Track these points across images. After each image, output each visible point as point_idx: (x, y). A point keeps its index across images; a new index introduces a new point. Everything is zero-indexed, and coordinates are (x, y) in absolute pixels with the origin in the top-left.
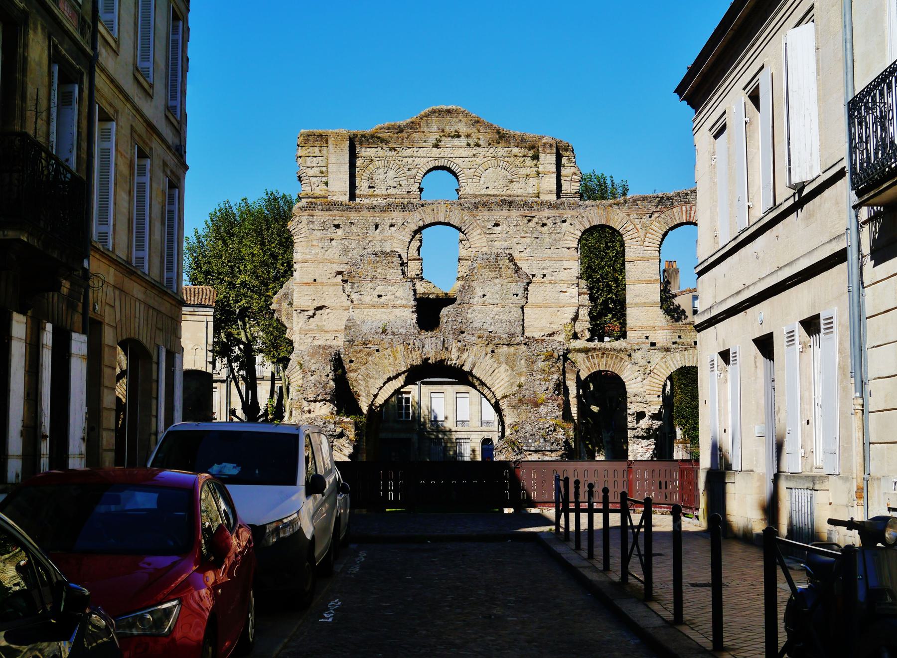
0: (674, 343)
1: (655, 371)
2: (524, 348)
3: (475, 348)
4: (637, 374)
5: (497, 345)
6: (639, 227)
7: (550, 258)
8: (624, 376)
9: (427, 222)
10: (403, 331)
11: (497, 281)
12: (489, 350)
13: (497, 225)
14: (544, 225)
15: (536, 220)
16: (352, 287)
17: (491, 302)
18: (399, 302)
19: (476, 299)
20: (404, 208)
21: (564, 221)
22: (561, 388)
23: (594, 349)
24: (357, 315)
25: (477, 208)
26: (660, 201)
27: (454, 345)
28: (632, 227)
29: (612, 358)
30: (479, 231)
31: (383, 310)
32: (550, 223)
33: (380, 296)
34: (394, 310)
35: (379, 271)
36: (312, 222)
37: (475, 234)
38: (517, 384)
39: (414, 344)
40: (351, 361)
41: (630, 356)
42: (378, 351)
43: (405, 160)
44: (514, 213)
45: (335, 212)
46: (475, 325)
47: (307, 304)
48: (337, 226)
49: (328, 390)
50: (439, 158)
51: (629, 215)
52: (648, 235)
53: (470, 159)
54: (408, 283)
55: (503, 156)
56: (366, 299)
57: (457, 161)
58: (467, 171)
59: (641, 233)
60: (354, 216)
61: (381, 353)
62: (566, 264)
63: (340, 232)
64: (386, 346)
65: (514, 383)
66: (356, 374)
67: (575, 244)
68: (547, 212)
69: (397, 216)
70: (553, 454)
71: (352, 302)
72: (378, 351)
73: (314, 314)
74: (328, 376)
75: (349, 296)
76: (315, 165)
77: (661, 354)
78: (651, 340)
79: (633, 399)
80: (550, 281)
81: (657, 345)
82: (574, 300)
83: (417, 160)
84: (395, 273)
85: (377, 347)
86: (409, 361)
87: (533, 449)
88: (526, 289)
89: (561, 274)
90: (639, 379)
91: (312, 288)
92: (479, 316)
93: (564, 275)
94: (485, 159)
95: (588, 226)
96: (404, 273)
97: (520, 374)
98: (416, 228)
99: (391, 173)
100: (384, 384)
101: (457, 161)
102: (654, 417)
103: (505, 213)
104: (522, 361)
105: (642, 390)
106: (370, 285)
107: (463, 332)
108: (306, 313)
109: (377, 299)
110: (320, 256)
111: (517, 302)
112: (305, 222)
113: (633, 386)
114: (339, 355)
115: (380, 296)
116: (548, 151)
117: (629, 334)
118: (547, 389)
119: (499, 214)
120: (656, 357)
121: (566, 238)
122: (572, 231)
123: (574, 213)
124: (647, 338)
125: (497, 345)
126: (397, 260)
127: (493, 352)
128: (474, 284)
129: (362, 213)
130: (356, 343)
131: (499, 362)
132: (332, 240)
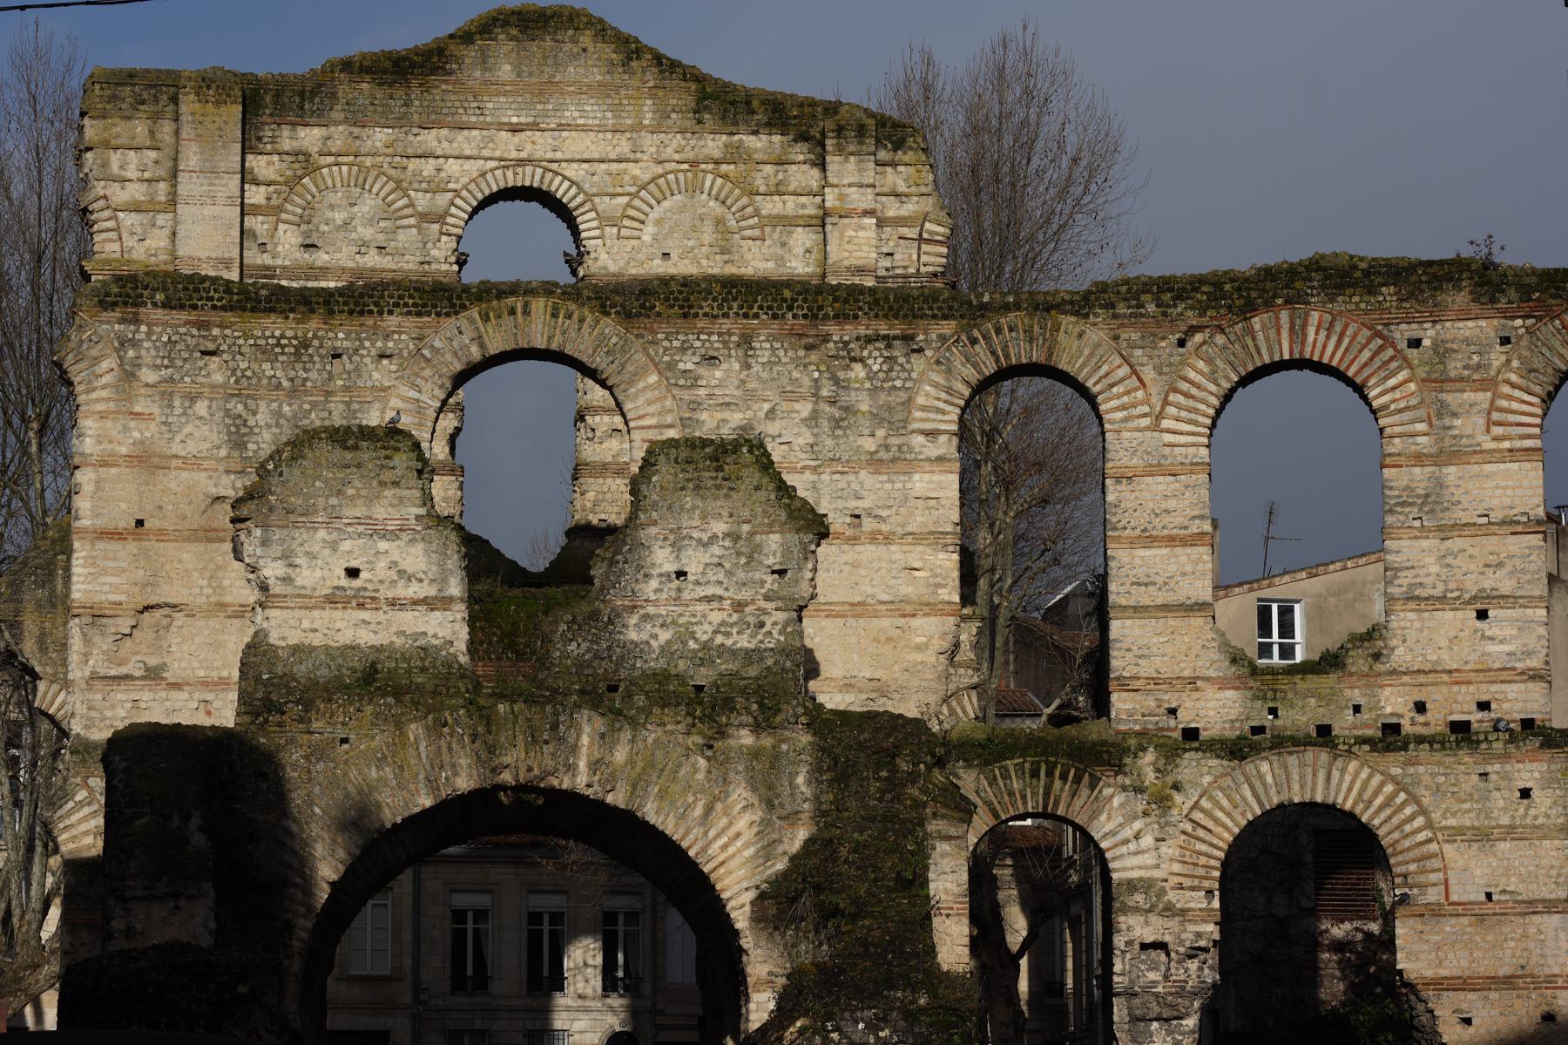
4: (1137, 825)
6: (1148, 373)
7: (875, 463)
8: (1102, 829)
9: (494, 349)
11: (720, 527)
13: (710, 360)
17: (701, 592)
18: (415, 590)
19: (654, 583)
24: (287, 628)
27: (587, 729)
31: (364, 615)
35: (350, 492)
43: (413, 165)
47: (114, 598)
50: (521, 162)
51: (1116, 338)
52: (1171, 398)
53: (614, 166)
58: (603, 203)
69: (400, 328)
78: (1186, 718)
81: (1204, 735)
83: (453, 166)
90: (1147, 841)
91: (132, 546)
95: (990, 368)
97: (792, 818)
98: (458, 366)
99: (368, 205)
101: (572, 171)
104: (800, 780)
113: (1128, 862)
115: (353, 573)
117: (1120, 702)
121: (920, 400)
124: (1172, 712)
126: (403, 461)
132: (193, 399)
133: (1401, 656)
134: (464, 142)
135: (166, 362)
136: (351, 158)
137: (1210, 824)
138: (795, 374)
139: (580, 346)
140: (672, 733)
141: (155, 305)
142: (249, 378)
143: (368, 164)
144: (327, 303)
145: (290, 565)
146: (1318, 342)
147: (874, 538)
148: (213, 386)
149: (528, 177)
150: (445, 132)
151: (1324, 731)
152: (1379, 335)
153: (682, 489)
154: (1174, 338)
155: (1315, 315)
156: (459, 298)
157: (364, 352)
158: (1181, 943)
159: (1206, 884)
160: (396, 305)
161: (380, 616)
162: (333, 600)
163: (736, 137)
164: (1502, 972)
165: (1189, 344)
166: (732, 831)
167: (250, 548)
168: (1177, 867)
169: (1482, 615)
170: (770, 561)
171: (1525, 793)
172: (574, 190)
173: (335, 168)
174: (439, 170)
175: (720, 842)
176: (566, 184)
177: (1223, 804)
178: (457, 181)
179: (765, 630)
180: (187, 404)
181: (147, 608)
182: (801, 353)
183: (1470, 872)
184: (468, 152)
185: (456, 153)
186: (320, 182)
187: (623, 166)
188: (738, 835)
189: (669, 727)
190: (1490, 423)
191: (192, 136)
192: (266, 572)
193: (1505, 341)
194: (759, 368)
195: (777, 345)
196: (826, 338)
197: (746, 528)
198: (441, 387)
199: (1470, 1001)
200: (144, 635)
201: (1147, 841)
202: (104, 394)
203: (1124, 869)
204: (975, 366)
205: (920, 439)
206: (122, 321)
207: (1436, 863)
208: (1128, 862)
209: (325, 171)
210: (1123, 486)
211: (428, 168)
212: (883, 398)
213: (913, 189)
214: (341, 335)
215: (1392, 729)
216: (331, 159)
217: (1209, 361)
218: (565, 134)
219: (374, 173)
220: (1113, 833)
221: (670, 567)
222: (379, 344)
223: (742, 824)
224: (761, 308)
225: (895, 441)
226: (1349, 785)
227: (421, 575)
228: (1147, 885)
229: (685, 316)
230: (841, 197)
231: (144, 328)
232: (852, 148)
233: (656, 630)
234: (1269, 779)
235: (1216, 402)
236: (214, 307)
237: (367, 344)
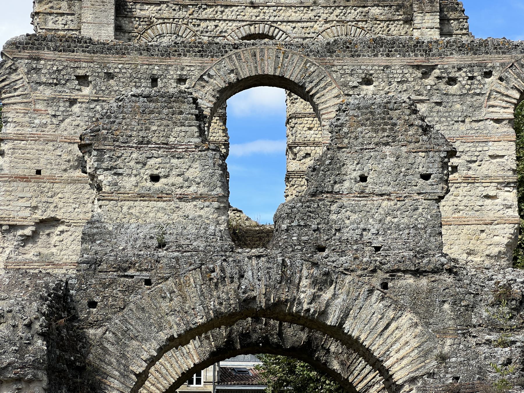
2: (449, 279)
3: (348, 279)
5: (393, 273)
9: (245, 73)
10: (200, 244)
11: (387, 150)
12: (376, 282)
13: (368, 81)
14: (452, 81)
15: (436, 72)
16: (100, 160)
19: (347, 184)
20: (201, 50)
21: (488, 74)
25: (331, 52)
27: (305, 273)
30: (335, 92)
31: (161, 204)
32: (462, 76)
33: (155, 178)
34: (182, 204)
36: (37, 70)
37: (328, 96)
38: (436, 352)
39: (223, 270)
40: (93, 304)
42: (148, 282)
43: (203, 25)
44: (397, 61)
45: (79, 55)
46: (346, 234)
48: (83, 80)
49: (29, 358)
53: (305, 25)
54: (210, 153)
55: (355, 20)
56: (128, 183)
57: (283, 27)
60: (114, 63)
61: (155, 288)
62: (493, 148)
63: (87, 91)
64: (166, 273)
65: (430, 351)
66: (100, 331)
67: (509, 113)
68: (455, 59)
69: (191, 64)
71: (99, 188)
72: (148, 282)
73: (35, 233)
74: (29, 326)
75: (93, 176)
76: (60, 27)
80: (467, 178)
83: (222, 26)
84: (185, 134)
85: (146, 275)
86: (212, 304)
89: (485, 165)
92: (354, 217)
93: (489, 168)
94: (328, 25)
96: (202, 133)
97: (444, 333)
98: (223, 85)
100: (162, 351)
101: (283, 27)
103: (382, 60)
104: (446, 306)
106: (134, 156)
107: (322, 249)
108: (20, 232)
109: (149, 184)
110: (49, 131)
111: (429, 189)
112: (22, 70)
114: (67, 290)
115: (155, 178)
116: (428, 9)
118: (509, 362)
119: (371, 63)
121: (491, 103)
122: (503, 90)
123: (507, 59)
125: (393, 273)
127: (385, 286)
128: (342, 155)
129: (127, 58)
130: (104, 266)
131: (402, 308)
132: (73, 102)
134: (229, 13)
135: (55, 81)
136: (172, 20)
138: (417, 88)
139: (293, 74)
140: (361, 276)
141: (49, 49)
142: (103, 91)
143: (180, 23)
144: (148, 50)
145: (115, 174)
148: (84, 96)
149: (260, 29)
150: (219, 8)
153: (362, 125)
156: (224, 47)
157: (170, 77)
160: (189, 51)
161: (173, 205)
162: (142, 196)
163: (366, 9)
166: (402, 341)
167: (91, 162)
170: (421, 169)
172: (284, 36)
173: (163, 25)
174: (216, 26)
175: (395, 347)
176: (281, 32)
178: (225, 32)
179: (417, 212)
180: (67, 104)
181: (42, 221)
182: (420, 75)
184: (230, 18)
185: (224, 18)
186: (155, 31)
187: (309, 24)
188: (407, 343)
189: (359, 272)
191: (89, 5)
192: (100, 178)
194: (395, 84)
195: (406, 71)
196: (434, 67)
197: (404, 149)
198: (213, 96)
200: (42, 238)
202: (18, 99)
205: (492, 122)
206: (31, 58)
209: (158, 26)
211: (211, 25)
212: (469, 98)
213: (459, 32)
214: (157, 68)
216: (161, 21)
218: (279, 8)
219: (184, 27)
221: (356, 174)
222: (179, 73)
223: (408, 336)
224: (396, 51)
225: (474, 125)
227: (198, 180)
229: (353, 56)
230: (422, 34)
231: (42, 62)
232: (428, 9)
233: (349, 213)
236: (83, 51)
237: (172, 73)
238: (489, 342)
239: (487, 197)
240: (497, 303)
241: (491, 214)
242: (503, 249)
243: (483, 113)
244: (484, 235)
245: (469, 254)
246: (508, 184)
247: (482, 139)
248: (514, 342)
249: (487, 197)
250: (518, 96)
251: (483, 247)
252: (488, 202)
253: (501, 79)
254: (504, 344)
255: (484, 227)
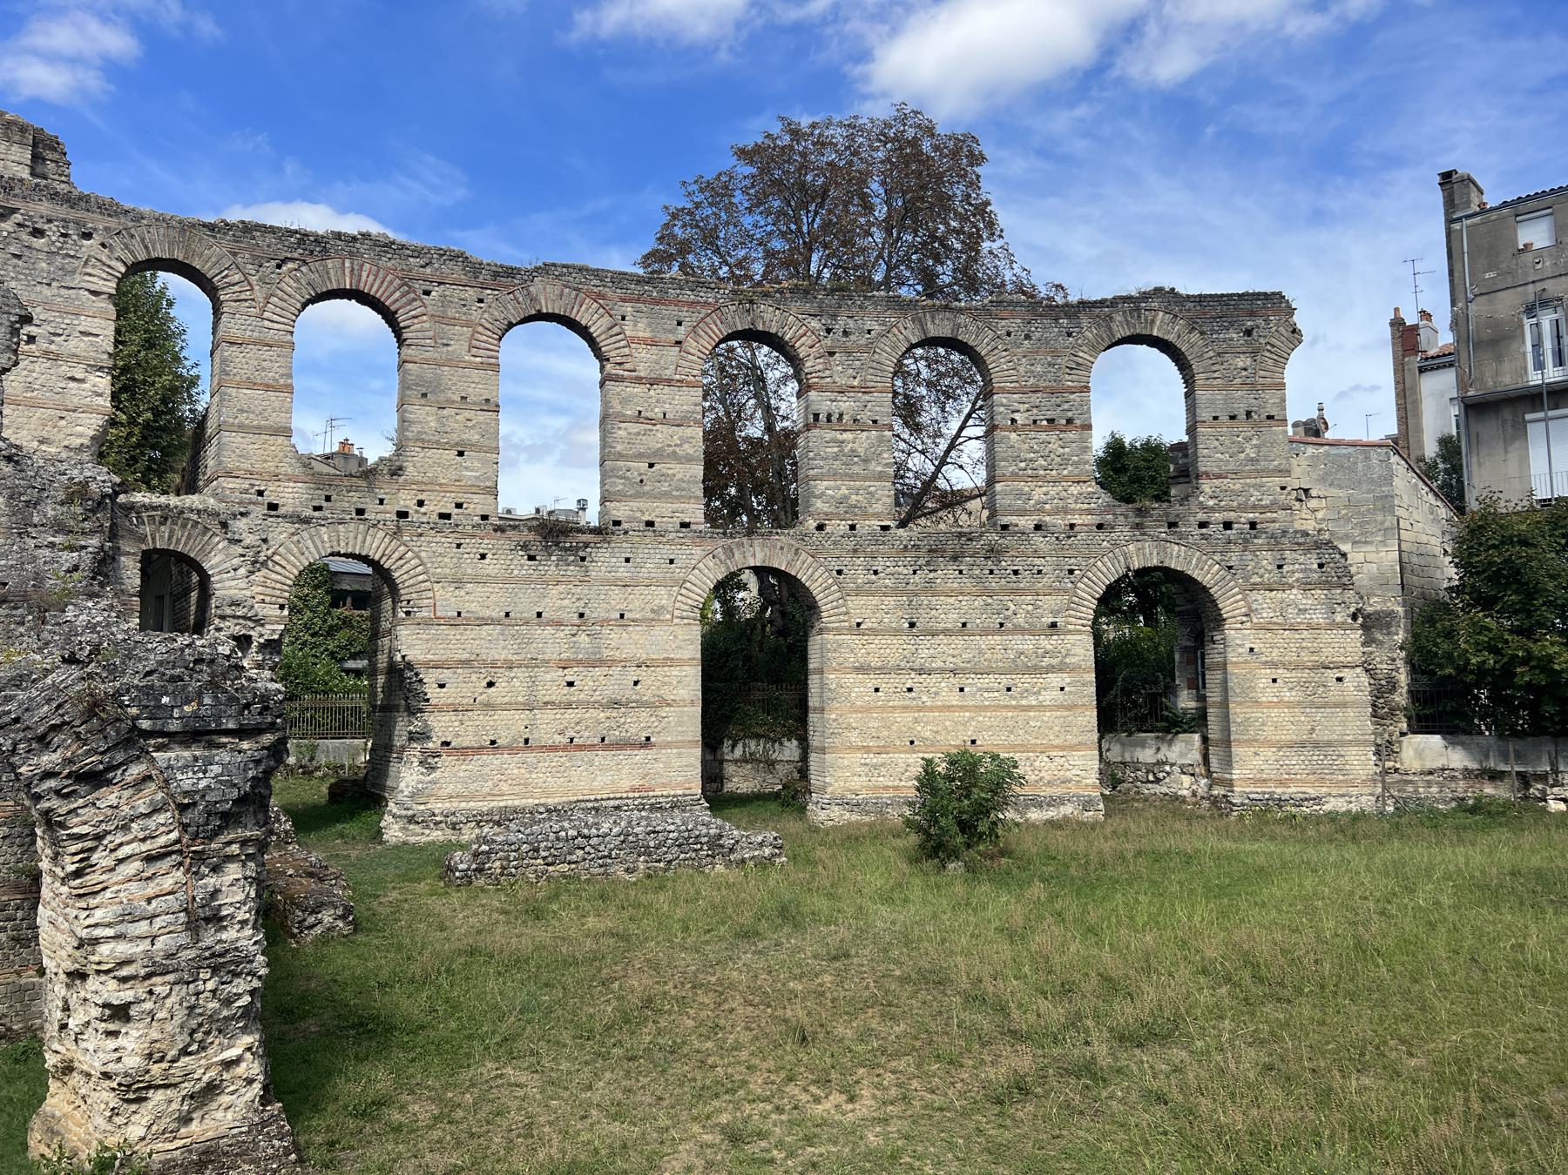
0: (316, 509)
1: (276, 558)
6: (253, 279)
8: (211, 564)
22: (104, 566)
23: (147, 507)
26: (301, 242)
28: (237, 277)
29: (184, 526)
41: (224, 525)
51: (235, 254)
52: (274, 300)
59: (259, 294)
62: (85, 324)
67: (110, 287)
70: (245, 745)
77: (291, 528)
79: (228, 611)
80: (46, 352)
81: (282, 511)
82: (100, 401)
87: (174, 726)
88: (15, 332)
89: (73, 343)
90: (242, 571)
93: (77, 345)
95: (142, 256)
102: (271, 646)
105: (248, 593)
118: (76, 568)
120: (280, 533)
123: (113, 223)
124: (260, 493)
133: (410, 471)
137: (284, 563)
146: (368, 284)
147: (46, 354)
151: (360, 512)
152: (406, 284)
154: (274, 263)
155: (367, 266)
158: (261, 635)
159: (281, 601)
164: (466, 656)
165: (284, 268)
168: (260, 589)
169: (461, 454)
171: (483, 557)
177: (293, 552)
183: (447, 600)
190: (471, 346)
193: (481, 301)
199: (444, 675)
201: (242, 571)
203: (224, 588)
204: (132, 252)
207: (430, 594)
208: (228, 584)
210: (235, 348)
212: (59, 259)
215: (402, 515)
217: (297, 281)
220: (217, 565)
225: (63, 292)
226: (376, 545)
228: (235, 604)
234: (326, 538)
235: (299, 306)
238: (52, 545)
239: (73, 379)
240: (68, 501)
241: (75, 400)
242: (86, 442)
243: (77, 280)
244: (63, 422)
245: (41, 442)
246: (101, 369)
247: (71, 309)
248: (85, 547)
249: (73, 379)
250: (123, 270)
251: (61, 436)
252: (72, 385)
253: (103, 245)
254: (72, 549)
255: (64, 414)
